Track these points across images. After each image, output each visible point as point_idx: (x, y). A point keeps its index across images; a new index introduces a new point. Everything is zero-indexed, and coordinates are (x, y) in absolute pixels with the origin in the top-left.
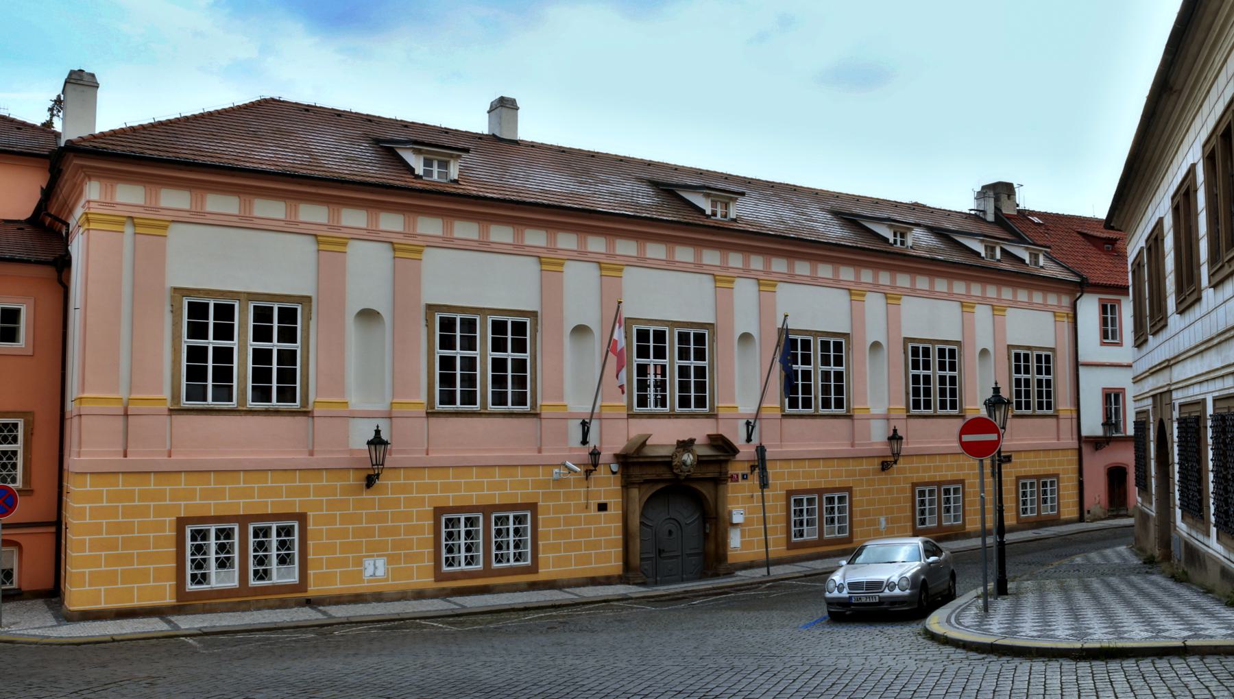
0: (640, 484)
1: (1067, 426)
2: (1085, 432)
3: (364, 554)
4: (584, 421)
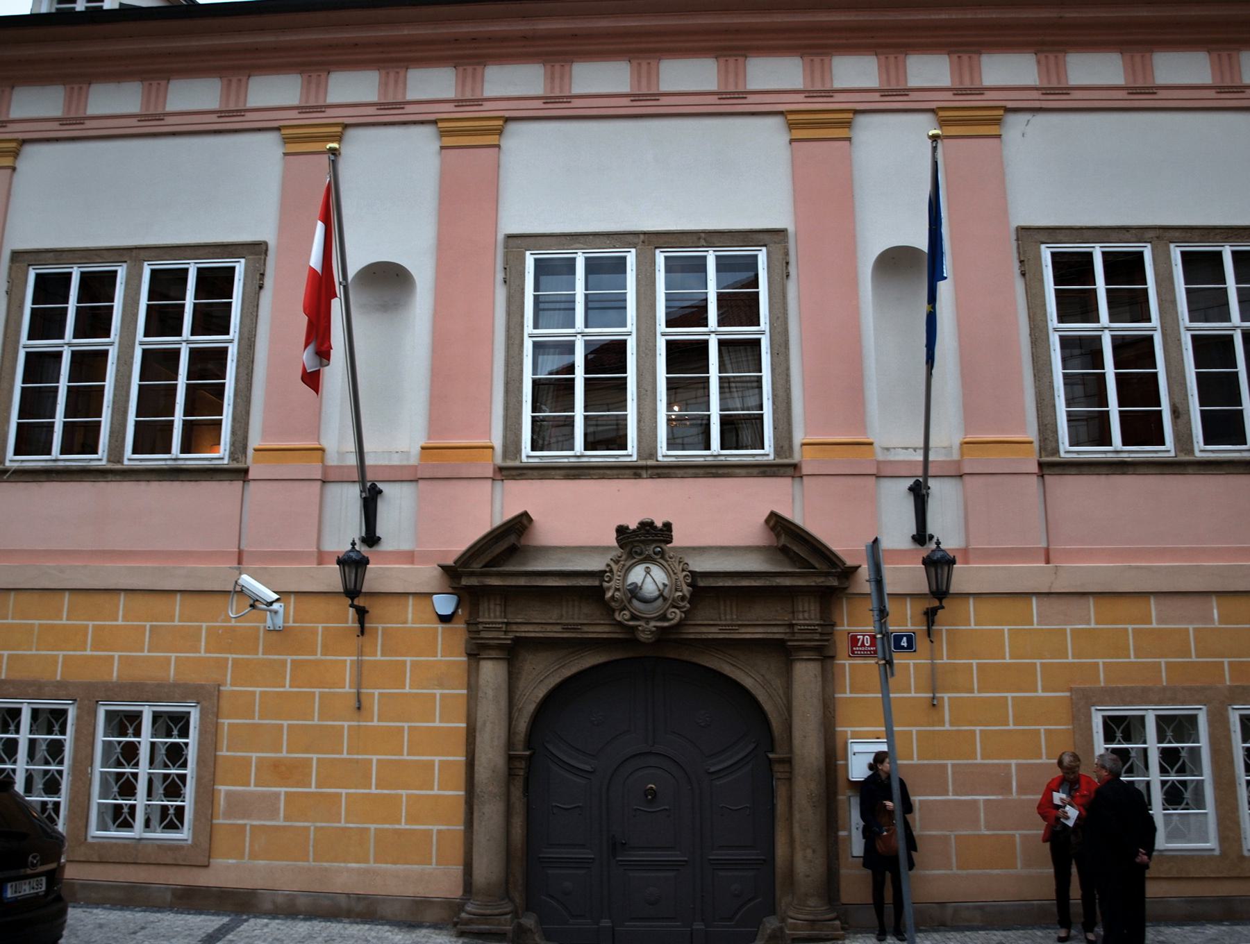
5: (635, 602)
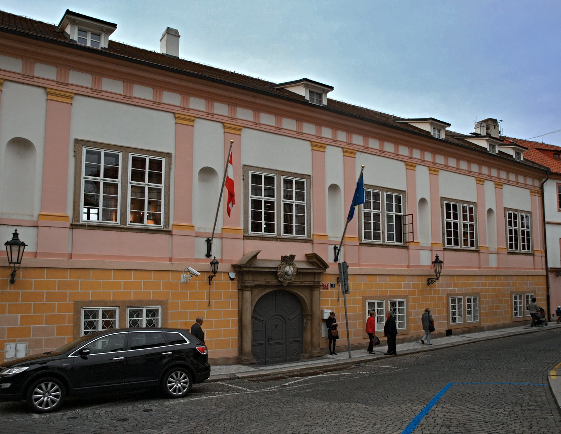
0: (252, 288)
1: (540, 260)
2: (550, 265)
3: (6, 339)
4: (208, 239)
5: (286, 276)
